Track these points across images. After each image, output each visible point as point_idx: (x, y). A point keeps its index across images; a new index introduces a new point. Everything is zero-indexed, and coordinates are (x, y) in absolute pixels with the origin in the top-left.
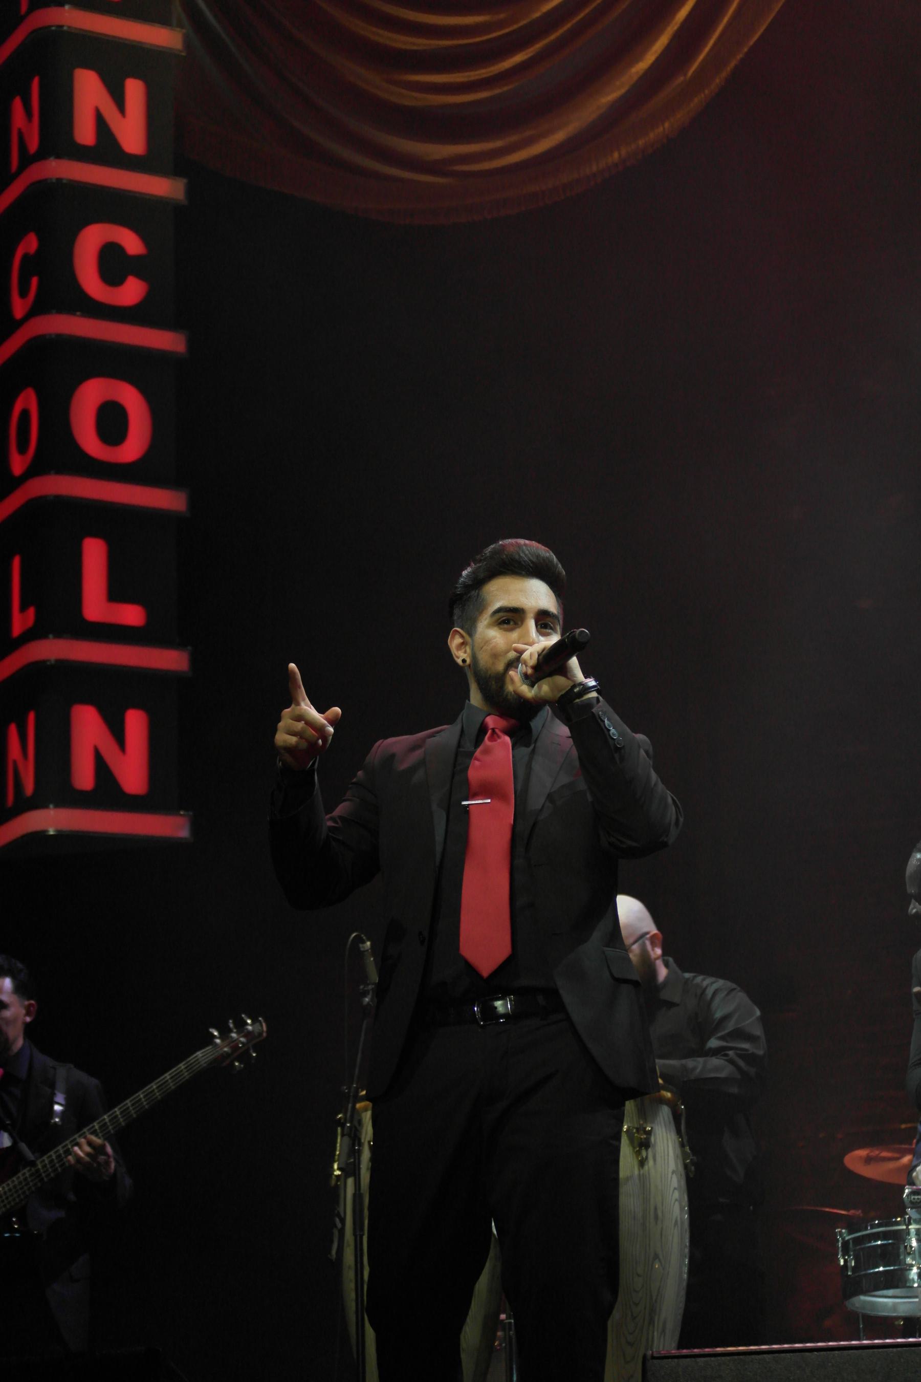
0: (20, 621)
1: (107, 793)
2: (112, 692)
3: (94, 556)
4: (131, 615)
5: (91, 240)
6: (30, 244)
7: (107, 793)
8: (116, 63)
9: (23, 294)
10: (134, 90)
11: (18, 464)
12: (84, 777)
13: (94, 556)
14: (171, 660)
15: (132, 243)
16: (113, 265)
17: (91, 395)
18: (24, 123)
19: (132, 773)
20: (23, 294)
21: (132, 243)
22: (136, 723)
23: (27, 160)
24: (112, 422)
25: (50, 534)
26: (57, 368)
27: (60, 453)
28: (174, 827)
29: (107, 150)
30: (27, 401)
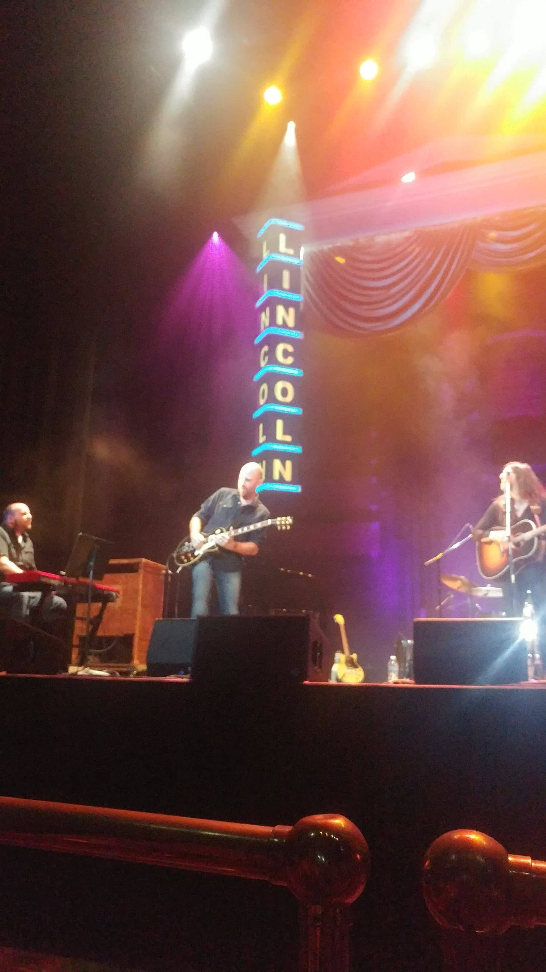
0: (262, 439)
1: (282, 480)
2: (284, 457)
3: (280, 424)
4: (288, 438)
5: (280, 348)
6: (266, 348)
7: (282, 480)
8: (287, 304)
9: (264, 359)
10: (292, 311)
11: (262, 402)
12: (276, 476)
13: (280, 424)
14: (297, 449)
15: (290, 348)
16: (286, 354)
17: (280, 386)
18: (265, 318)
19: (288, 476)
20: (264, 359)
21: (290, 348)
22: (289, 464)
23: (265, 328)
24: (284, 392)
25: (269, 419)
26: (272, 379)
27: (272, 399)
28: (296, 489)
29: (285, 325)
30: (264, 387)
